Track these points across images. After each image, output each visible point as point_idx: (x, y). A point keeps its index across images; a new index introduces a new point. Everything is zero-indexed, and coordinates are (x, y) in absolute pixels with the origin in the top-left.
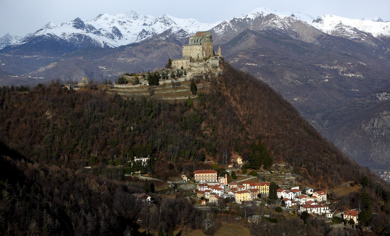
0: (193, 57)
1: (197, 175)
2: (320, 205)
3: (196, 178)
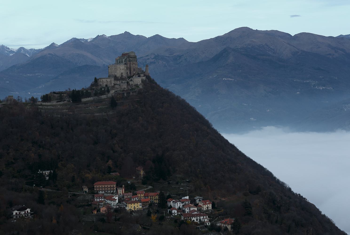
2: (201, 212)
3: (95, 189)
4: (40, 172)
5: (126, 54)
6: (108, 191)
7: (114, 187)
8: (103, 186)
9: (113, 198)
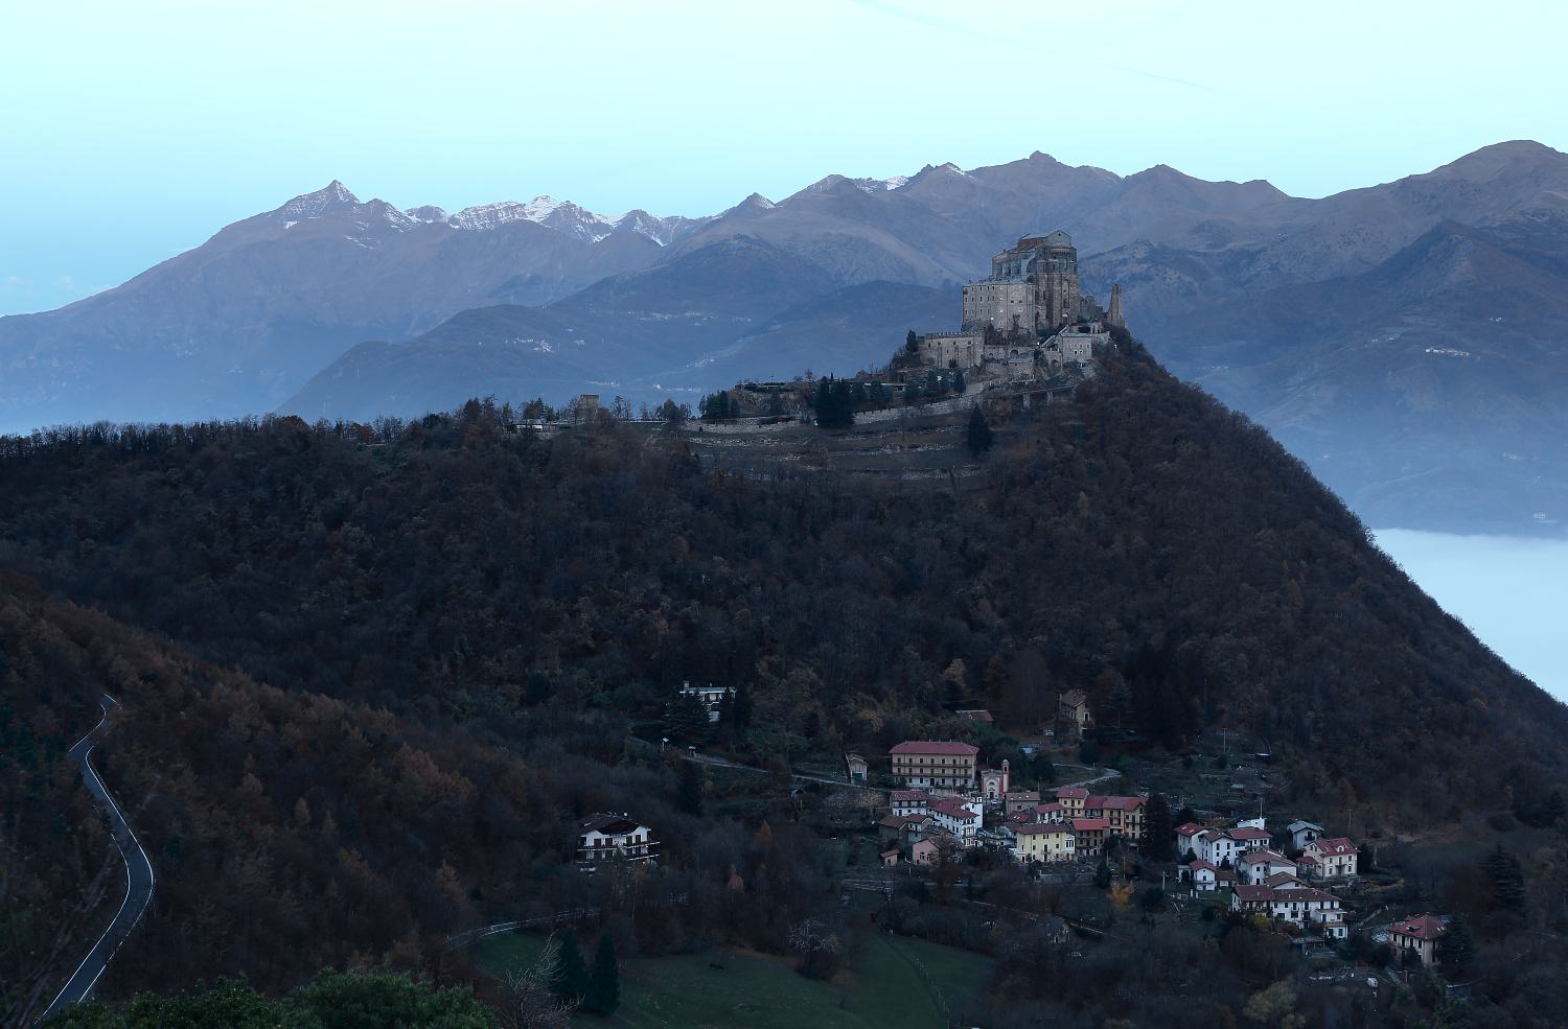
1: (899, 760)
3: (895, 770)
4: (687, 689)
5: (1035, 241)
6: (943, 782)
7: (967, 767)
8: (927, 760)
9: (963, 807)
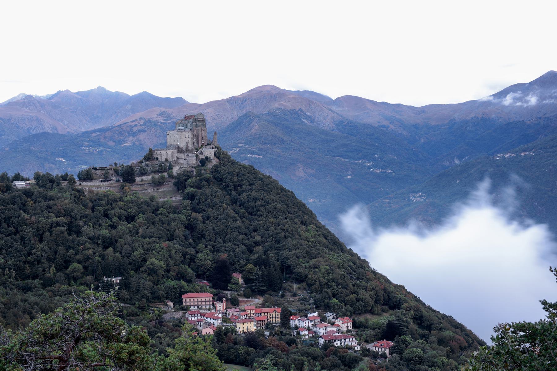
0: (181, 146)
3: (184, 304)
5: (192, 116)
8: (196, 300)
